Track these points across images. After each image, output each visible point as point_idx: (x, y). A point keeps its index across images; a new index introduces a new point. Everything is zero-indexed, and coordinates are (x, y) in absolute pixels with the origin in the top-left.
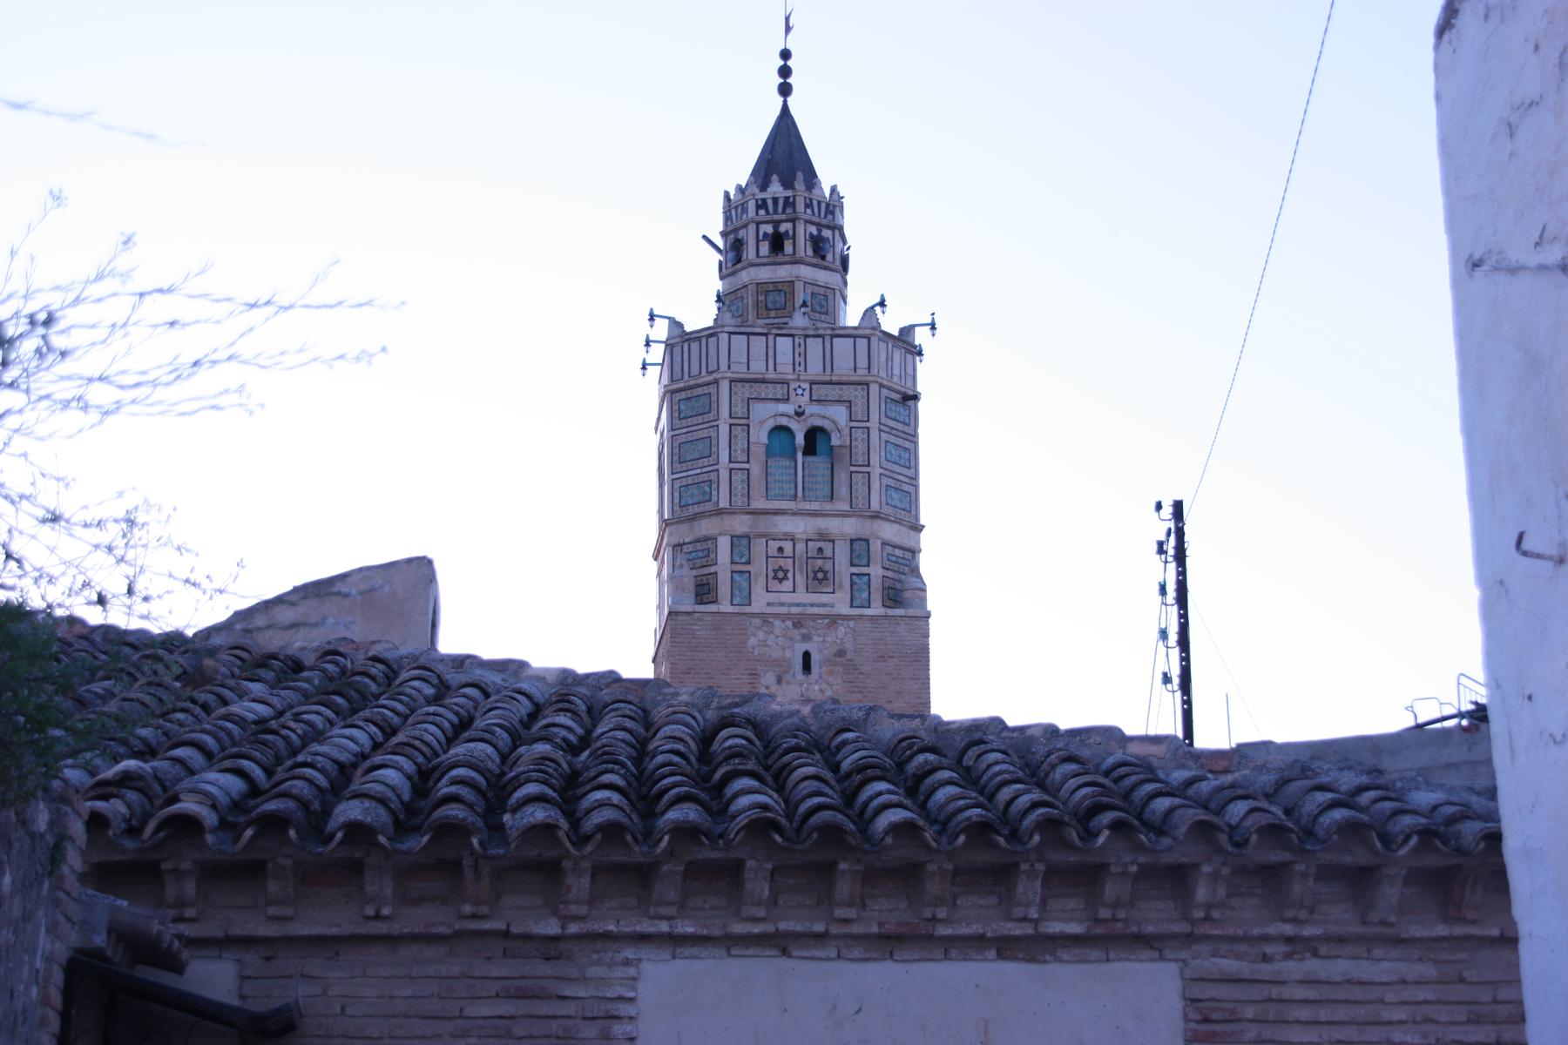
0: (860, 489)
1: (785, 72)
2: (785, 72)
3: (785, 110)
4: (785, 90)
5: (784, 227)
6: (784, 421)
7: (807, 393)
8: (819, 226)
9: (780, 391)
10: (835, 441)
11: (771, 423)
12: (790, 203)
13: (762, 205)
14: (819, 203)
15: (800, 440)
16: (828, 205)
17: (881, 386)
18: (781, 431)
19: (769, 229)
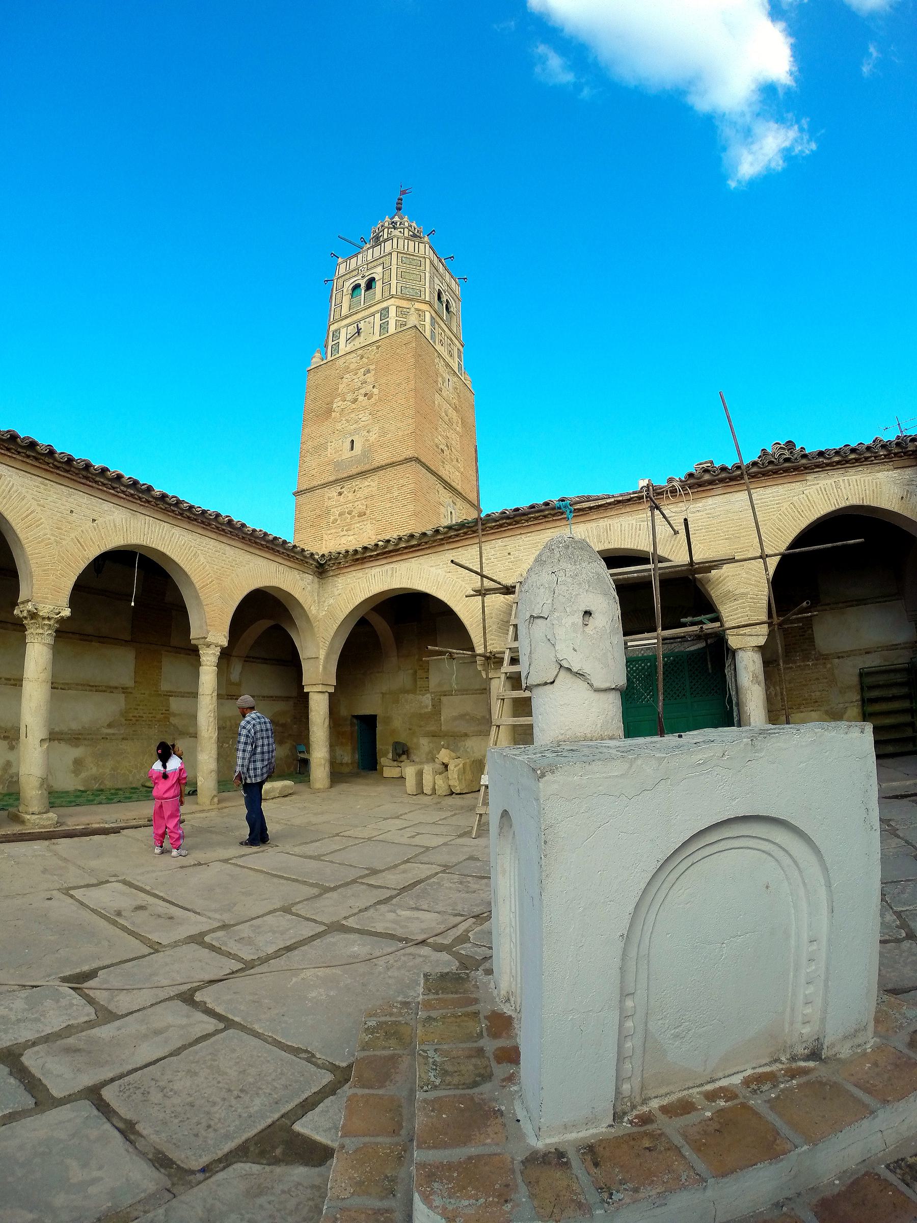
9: (355, 273)
15: (363, 286)
17: (398, 252)
18: (357, 286)
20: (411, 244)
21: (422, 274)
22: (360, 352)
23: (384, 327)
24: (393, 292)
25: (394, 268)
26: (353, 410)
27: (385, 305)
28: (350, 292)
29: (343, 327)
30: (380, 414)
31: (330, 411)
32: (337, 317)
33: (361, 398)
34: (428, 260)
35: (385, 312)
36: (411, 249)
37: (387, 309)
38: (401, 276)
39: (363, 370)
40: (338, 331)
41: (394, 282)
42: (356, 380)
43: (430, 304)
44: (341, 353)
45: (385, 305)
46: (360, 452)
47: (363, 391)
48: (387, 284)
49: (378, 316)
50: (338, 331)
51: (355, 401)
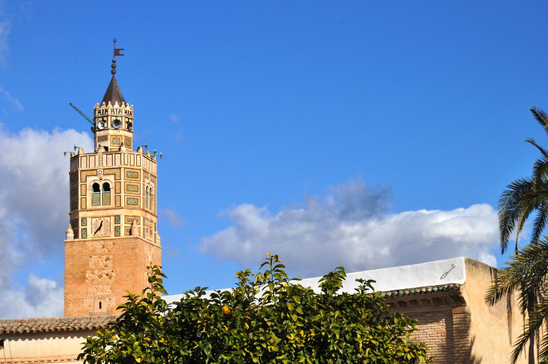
1: (113, 67)
4: (113, 73)
5: (105, 119)
8: (117, 116)
9: (94, 173)
10: (111, 187)
11: (93, 183)
12: (106, 111)
13: (99, 112)
14: (117, 109)
17: (125, 168)
20: (132, 156)
21: (139, 185)
22: (102, 242)
23: (117, 230)
24: (123, 205)
25: (123, 181)
26: (100, 283)
27: (117, 212)
28: (92, 188)
29: (89, 217)
30: (117, 290)
31: (83, 278)
33: (104, 276)
35: (117, 218)
36: (132, 164)
38: (128, 189)
39: (105, 257)
40: (84, 219)
41: (123, 194)
42: (101, 263)
43: (143, 210)
45: (117, 212)
46: (105, 311)
47: (106, 272)
48: (118, 193)
49: (113, 218)
50: (84, 219)
51: (100, 276)
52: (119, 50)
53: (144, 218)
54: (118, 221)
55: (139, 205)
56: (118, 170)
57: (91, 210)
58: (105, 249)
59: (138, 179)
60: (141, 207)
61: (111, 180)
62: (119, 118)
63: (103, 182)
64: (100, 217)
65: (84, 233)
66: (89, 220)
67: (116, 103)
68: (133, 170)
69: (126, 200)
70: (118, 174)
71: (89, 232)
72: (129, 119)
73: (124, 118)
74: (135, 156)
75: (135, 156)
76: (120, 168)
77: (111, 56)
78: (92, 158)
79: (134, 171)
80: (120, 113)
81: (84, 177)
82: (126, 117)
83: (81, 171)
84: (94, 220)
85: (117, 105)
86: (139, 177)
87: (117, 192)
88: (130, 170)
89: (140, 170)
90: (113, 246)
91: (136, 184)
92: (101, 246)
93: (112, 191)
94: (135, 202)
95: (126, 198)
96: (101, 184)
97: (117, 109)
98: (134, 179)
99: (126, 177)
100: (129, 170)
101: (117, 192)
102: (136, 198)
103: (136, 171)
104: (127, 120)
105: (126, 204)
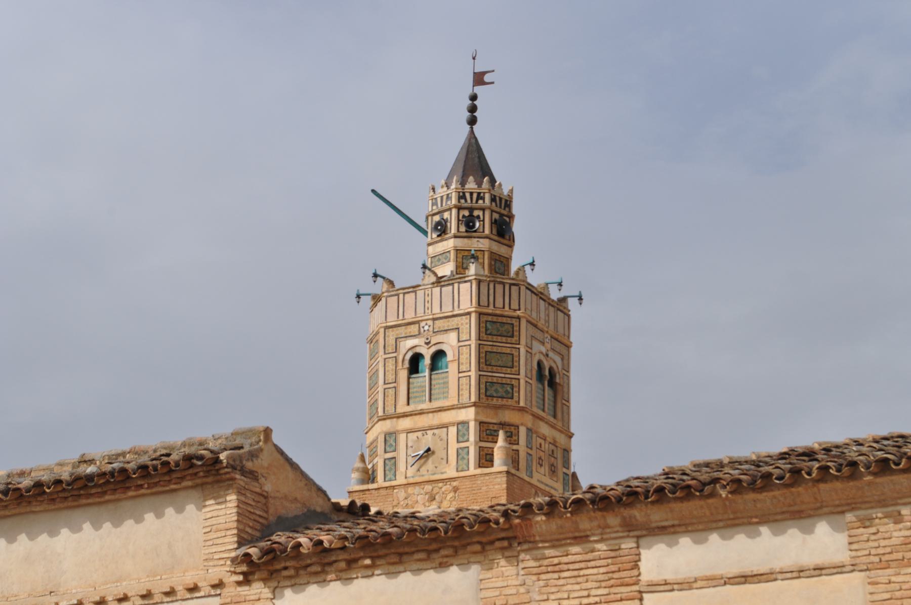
0: (465, 387)
1: (473, 109)
2: (473, 109)
3: (472, 132)
4: (472, 121)
5: (446, 215)
6: (418, 350)
7: (431, 329)
8: (471, 210)
9: (414, 329)
10: (450, 356)
12: (448, 197)
14: (471, 194)
15: (427, 361)
16: (479, 194)
19: (437, 218)
20: (499, 288)
21: (516, 354)
22: (428, 488)
28: (407, 365)
29: (403, 431)
32: (390, 410)
34: (524, 323)
37: (465, 423)
44: (401, 480)
49: (453, 430)
52: (484, 73)
53: (529, 430)
54: (464, 435)
55: (516, 398)
56: (465, 319)
57: (405, 415)
58: (434, 503)
59: (514, 340)
60: (522, 404)
61: (449, 343)
62: (476, 213)
63: (433, 349)
64: (424, 430)
65: (390, 470)
66: (402, 437)
67: (471, 178)
68: (500, 319)
69: (483, 386)
70: (464, 328)
71: (401, 466)
72: (501, 215)
73: (487, 213)
74: (507, 287)
75: (507, 287)
76: (469, 314)
77: (468, 88)
78: (410, 298)
79: (504, 320)
80: (481, 202)
81: (391, 340)
82: (492, 211)
83: (386, 328)
84: (412, 436)
85: (471, 185)
86: (516, 333)
87: (464, 368)
88: (495, 319)
89: (519, 318)
90: (452, 494)
91: (508, 351)
92: (427, 497)
93: (452, 369)
94: (507, 392)
95: (484, 380)
96: (427, 353)
97: (471, 194)
98: (504, 339)
99: (483, 335)
100: (490, 318)
101: (463, 368)
102: (508, 381)
103: (509, 321)
104: (496, 216)
105: (483, 396)
